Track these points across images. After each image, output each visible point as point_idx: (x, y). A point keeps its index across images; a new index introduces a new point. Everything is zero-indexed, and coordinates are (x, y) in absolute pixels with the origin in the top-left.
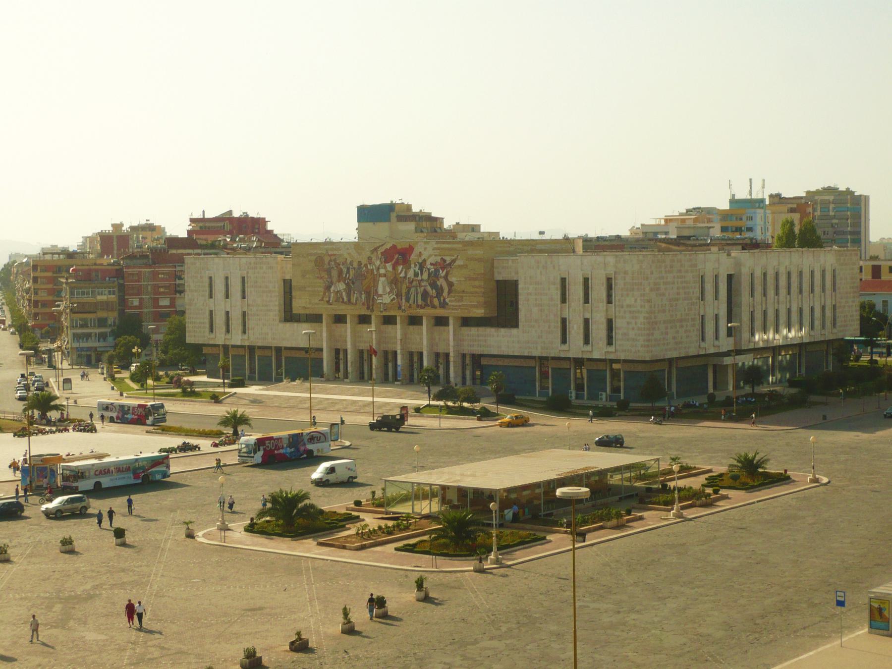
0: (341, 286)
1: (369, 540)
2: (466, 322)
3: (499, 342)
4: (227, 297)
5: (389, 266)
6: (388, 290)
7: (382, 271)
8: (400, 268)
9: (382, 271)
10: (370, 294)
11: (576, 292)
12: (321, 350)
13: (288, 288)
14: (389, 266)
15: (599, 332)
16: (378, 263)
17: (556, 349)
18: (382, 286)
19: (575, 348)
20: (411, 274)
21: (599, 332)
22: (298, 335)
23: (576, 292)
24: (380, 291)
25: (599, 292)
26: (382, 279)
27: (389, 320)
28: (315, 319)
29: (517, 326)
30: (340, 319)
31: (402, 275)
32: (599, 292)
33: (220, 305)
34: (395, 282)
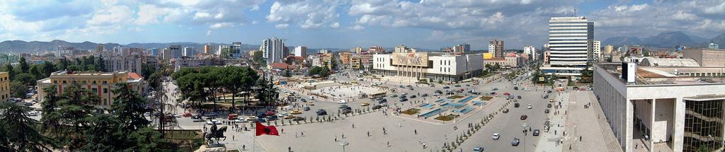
1: (426, 116)
2: (423, 67)
3: (430, 71)
10: (406, 62)
11: (443, 63)
13: (391, 60)
15: (447, 70)
17: (439, 73)
18: (409, 60)
19: (443, 73)
21: (447, 70)
22: (393, 68)
23: (443, 63)
25: (447, 63)
27: (410, 67)
28: (397, 66)
29: (432, 68)
32: (447, 63)
33: (379, 63)
34: (411, 60)
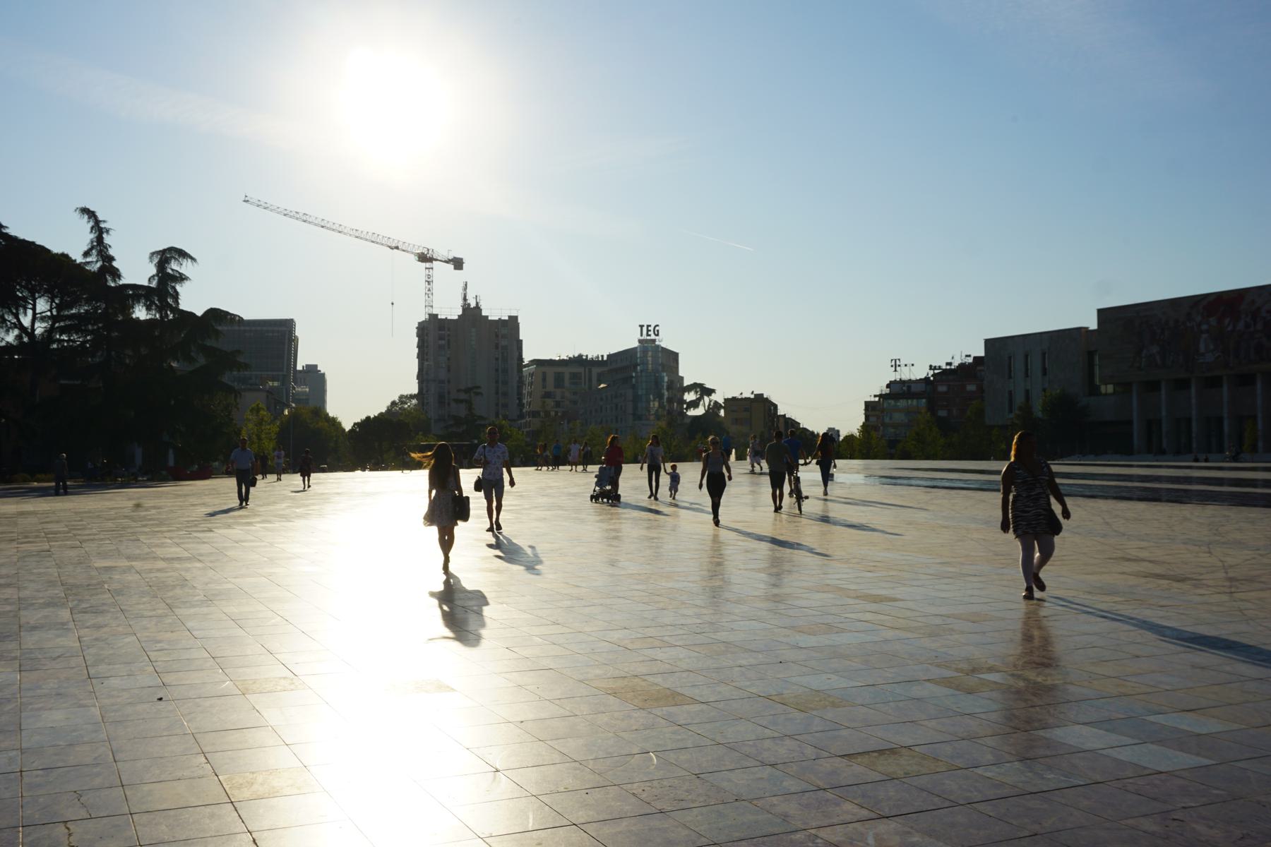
0: (1155, 349)
4: (1027, 375)
5: (1213, 321)
6: (1212, 347)
7: (1204, 327)
8: (1227, 321)
9: (1204, 327)
12: (1130, 423)
14: (1213, 321)
16: (1199, 318)
20: (1241, 326)
24: (1202, 348)
26: (1204, 336)
27: (1214, 383)
30: (1153, 386)
31: (1230, 328)
